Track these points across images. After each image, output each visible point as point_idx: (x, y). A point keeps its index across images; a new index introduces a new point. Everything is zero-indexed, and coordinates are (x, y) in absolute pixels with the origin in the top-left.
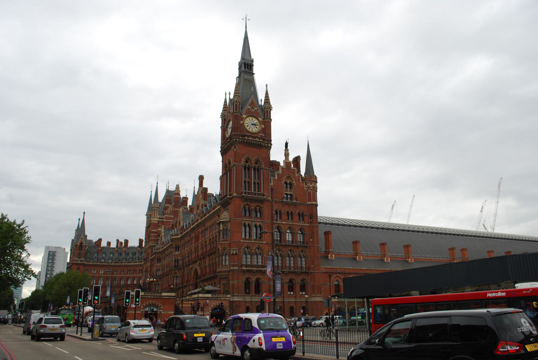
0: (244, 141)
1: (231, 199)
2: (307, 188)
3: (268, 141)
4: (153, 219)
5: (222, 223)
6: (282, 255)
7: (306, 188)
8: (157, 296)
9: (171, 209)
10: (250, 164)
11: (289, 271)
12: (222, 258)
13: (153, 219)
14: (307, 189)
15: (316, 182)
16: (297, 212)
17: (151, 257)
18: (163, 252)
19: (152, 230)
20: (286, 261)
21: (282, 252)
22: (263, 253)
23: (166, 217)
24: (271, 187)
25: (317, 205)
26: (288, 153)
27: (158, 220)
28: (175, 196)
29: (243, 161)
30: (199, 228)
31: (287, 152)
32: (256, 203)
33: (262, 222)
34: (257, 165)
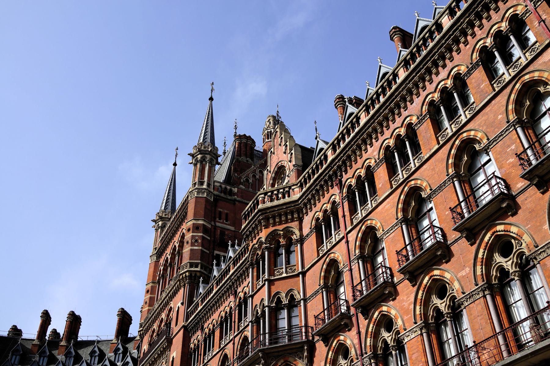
27: (216, 193)
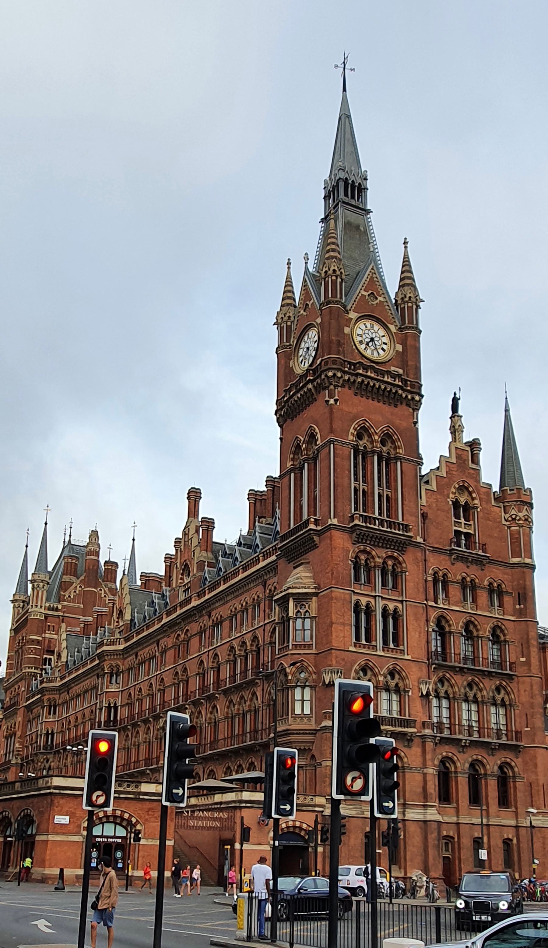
0: (354, 381)
1: (319, 533)
2: (510, 521)
3: (412, 386)
4: (34, 609)
5: (294, 599)
6: (451, 696)
7: (506, 521)
8: (129, 793)
9: (78, 588)
10: (369, 446)
11: (471, 741)
12: (293, 695)
13: (34, 609)
14: (508, 523)
15: (531, 506)
16: (486, 583)
17: (26, 702)
18: (66, 687)
19: (31, 637)
20: (462, 712)
21: (450, 688)
22: (406, 686)
23: (63, 607)
24: (421, 510)
25: (532, 567)
26: (459, 426)
28: (88, 557)
29: (353, 434)
30: (189, 623)
31: (459, 423)
32: (387, 548)
33: (402, 602)
34: (385, 449)
